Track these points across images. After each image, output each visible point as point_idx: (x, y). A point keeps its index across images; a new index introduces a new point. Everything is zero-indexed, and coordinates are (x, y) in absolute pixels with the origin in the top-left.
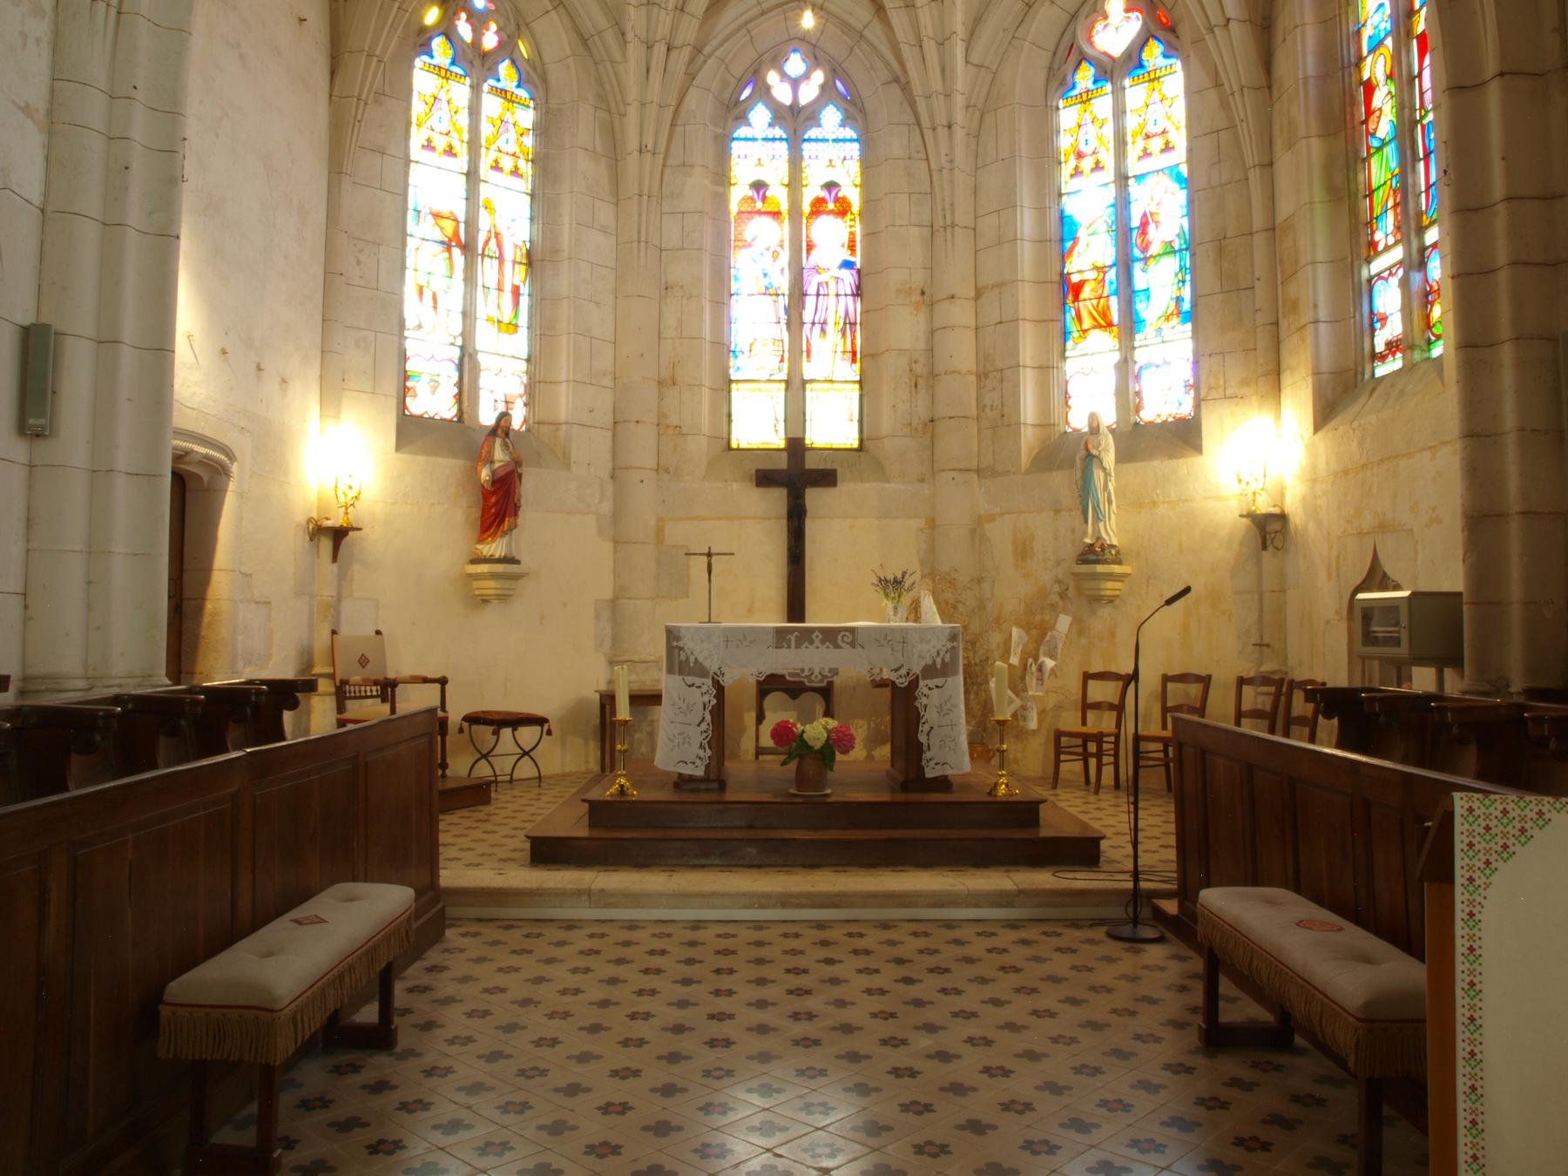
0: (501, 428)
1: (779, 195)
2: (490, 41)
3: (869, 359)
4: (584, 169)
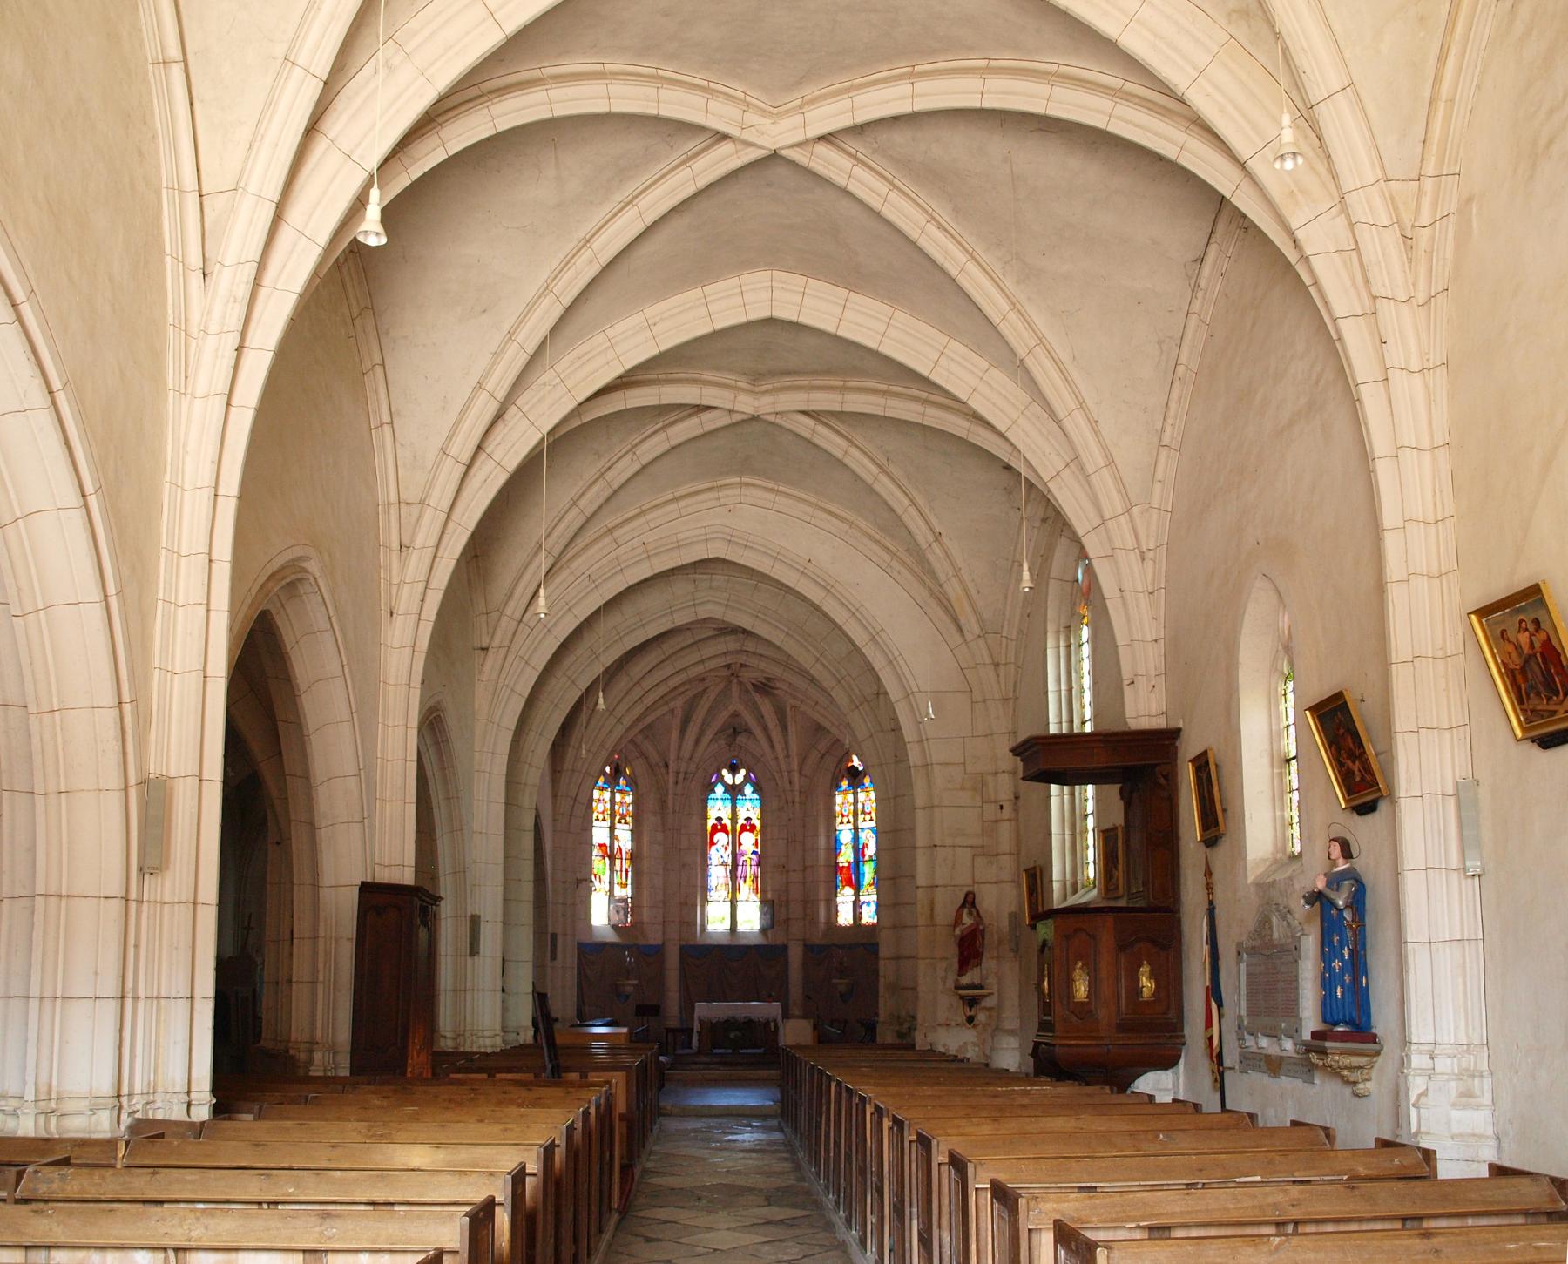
4: (650, 820)
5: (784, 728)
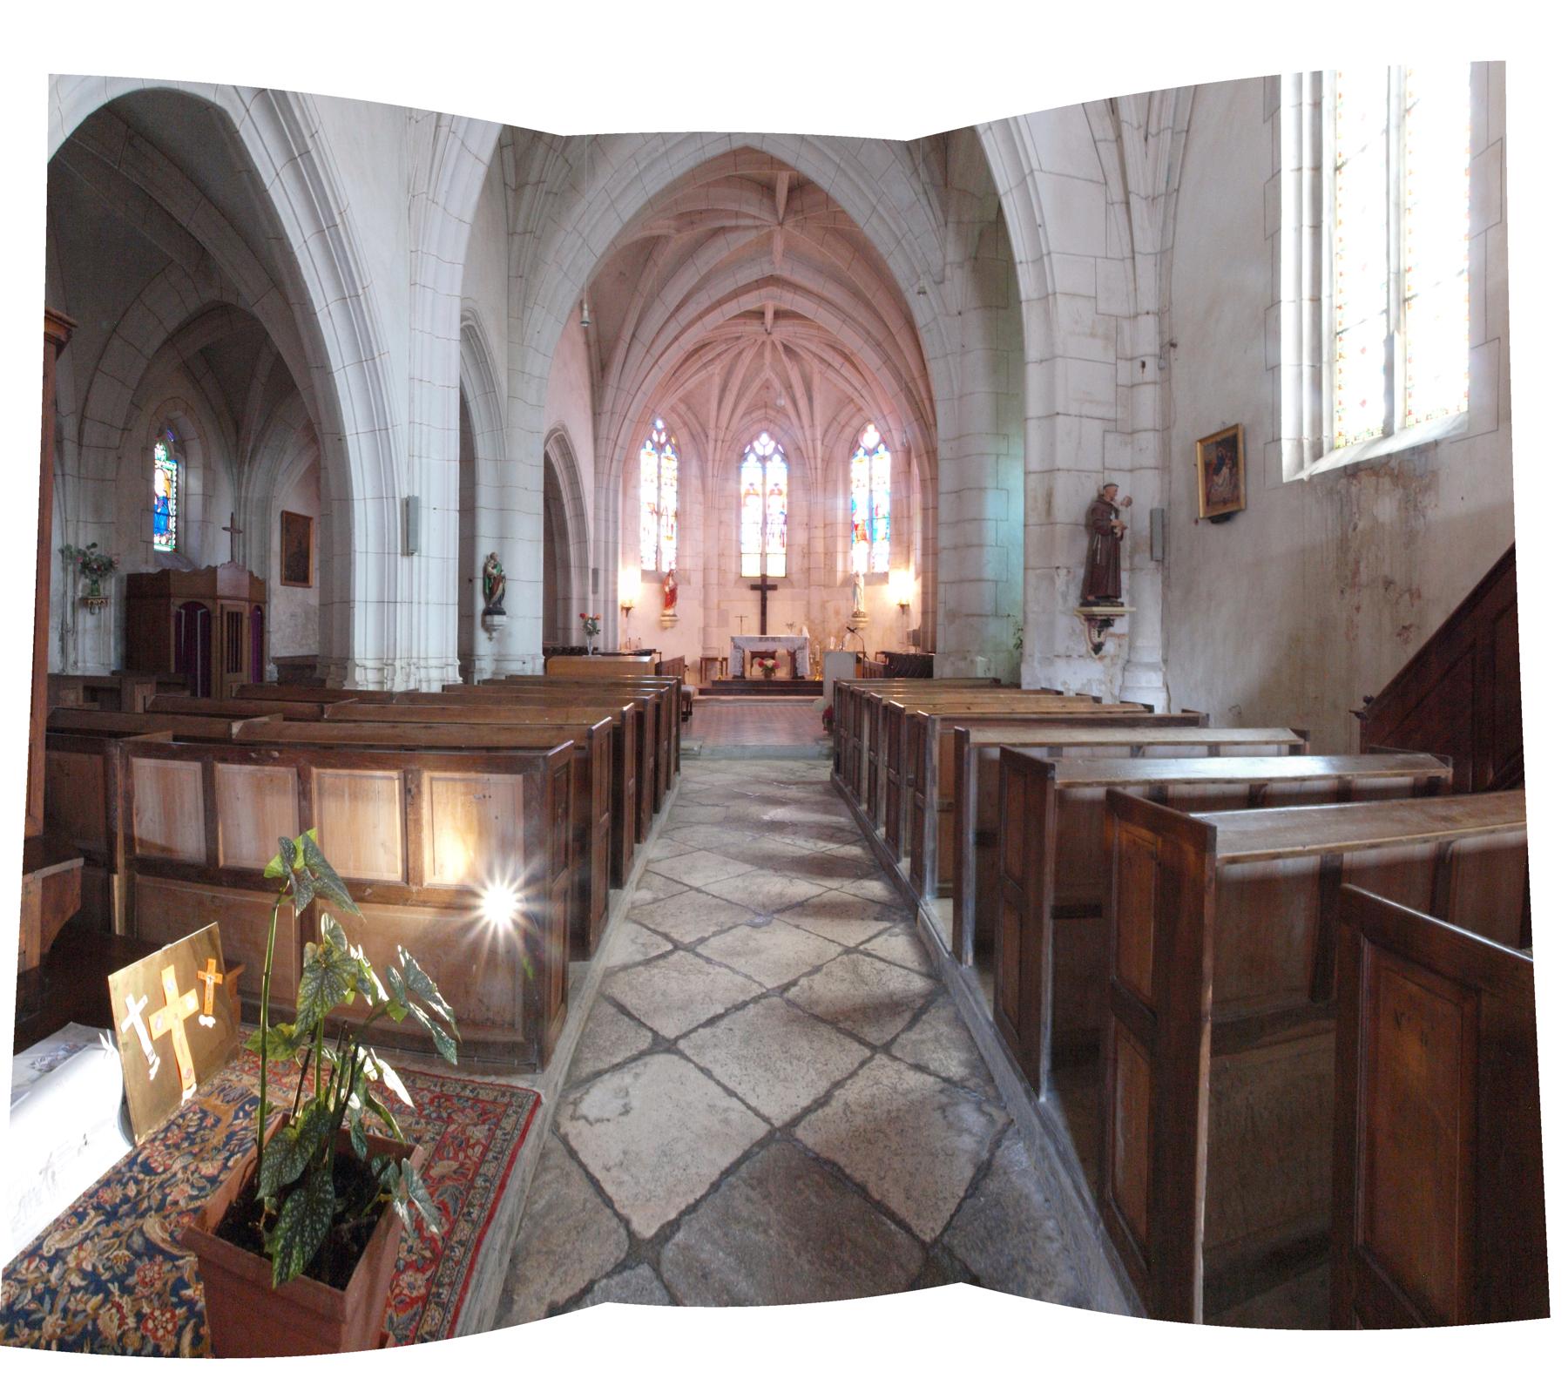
0: (670, 574)
1: (759, 490)
2: (663, 439)
3: (789, 546)
5: (810, 399)
